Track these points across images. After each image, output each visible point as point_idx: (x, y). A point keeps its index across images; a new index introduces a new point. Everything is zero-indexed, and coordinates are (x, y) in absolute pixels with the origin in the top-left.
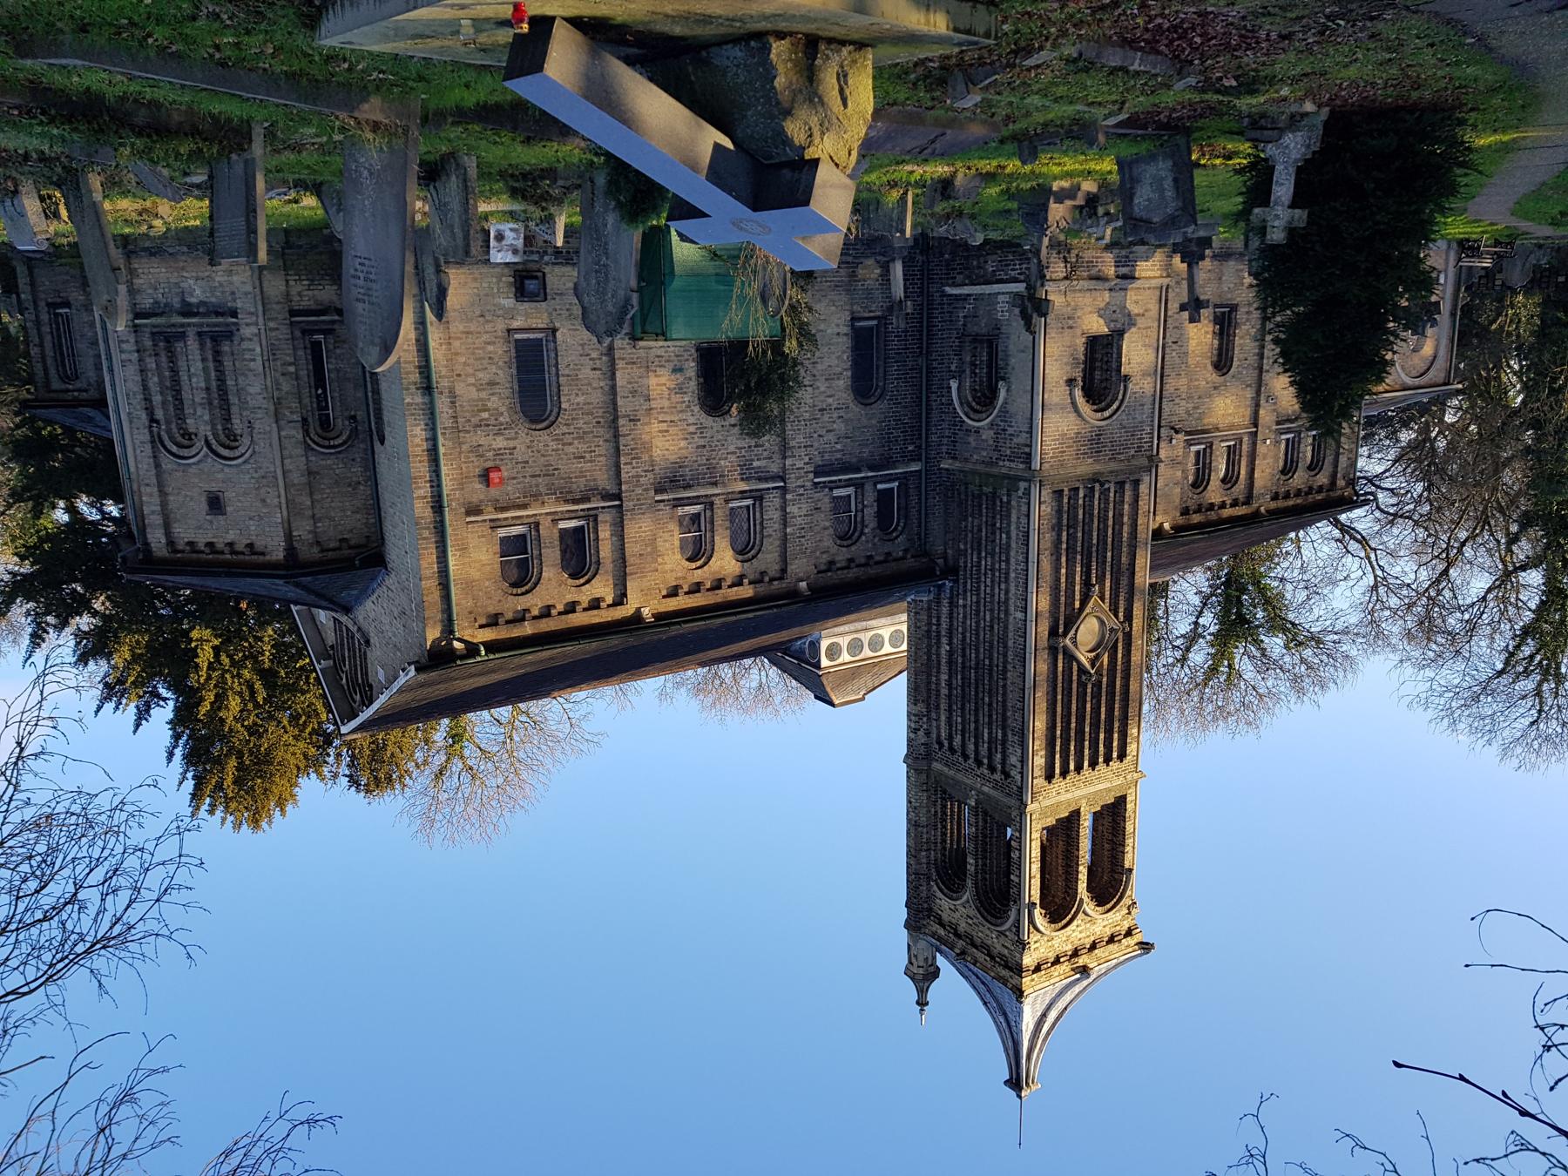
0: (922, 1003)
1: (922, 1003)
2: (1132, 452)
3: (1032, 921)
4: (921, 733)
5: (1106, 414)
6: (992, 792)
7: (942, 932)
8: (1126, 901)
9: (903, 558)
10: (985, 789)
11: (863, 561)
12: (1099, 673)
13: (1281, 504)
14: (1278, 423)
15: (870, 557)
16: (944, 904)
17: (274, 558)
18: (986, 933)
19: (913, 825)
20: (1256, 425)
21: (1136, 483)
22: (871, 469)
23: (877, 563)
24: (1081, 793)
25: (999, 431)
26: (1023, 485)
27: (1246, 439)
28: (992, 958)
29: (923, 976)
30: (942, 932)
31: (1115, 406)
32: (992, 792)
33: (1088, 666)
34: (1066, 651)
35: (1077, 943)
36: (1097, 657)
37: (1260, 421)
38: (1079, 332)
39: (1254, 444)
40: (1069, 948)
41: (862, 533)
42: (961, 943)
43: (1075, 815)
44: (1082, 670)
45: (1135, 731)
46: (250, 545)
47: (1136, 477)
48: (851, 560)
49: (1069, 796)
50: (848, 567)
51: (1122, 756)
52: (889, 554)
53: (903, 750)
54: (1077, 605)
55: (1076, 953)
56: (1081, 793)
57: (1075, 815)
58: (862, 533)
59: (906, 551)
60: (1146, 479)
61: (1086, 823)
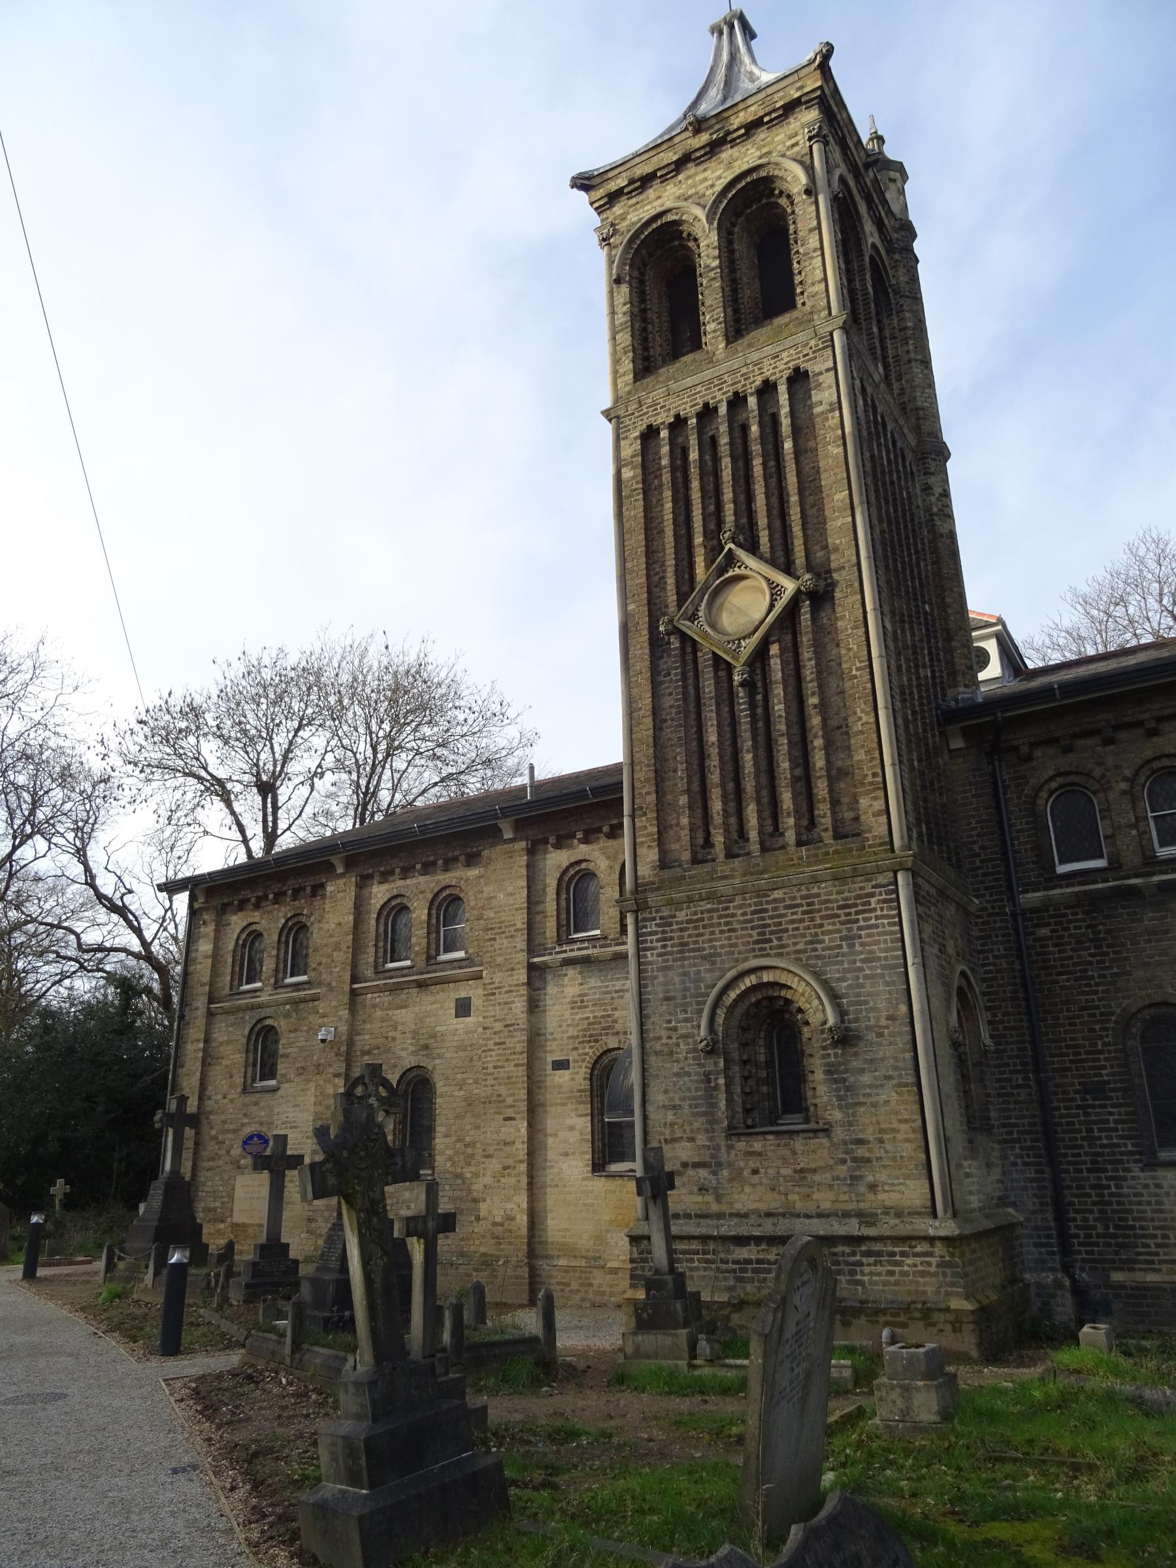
2: (682, 916)
3: (809, 169)
4: (938, 490)
5: (749, 981)
8: (620, 240)
9: (1033, 745)
11: (1122, 735)
12: (714, 549)
13: (309, 882)
14: (315, 998)
15: (1110, 741)
19: (926, 363)
20: (354, 993)
21: (664, 863)
22: (1134, 891)
23: (1096, 732)
24: (723, 368)
27: (369, 973)
31: (733, 995)
33: (741, 554)
34: (788, 569)
35: (712, 164)
36: (722, 570)
37: (346, 999)
38: (839, 1133)
39: (354, 965)
40: (727, 154)
41: (1132, 780)
43: (735, 331)
44: (753, 548)
45: (627, 473)
47: (667, 874)
48: (1153, 733)
49: (755, 356)
50: (1160, 719)
51: (649, 435)
52: (1067, 750)
53: (954, 468)
54: (774, 649)
55: (714, 148)
56: (723, 368)
57: (735, 331)
58: (1132, 780)
59: (1030, 758)
60: (645, 871)
61: (712, 322)
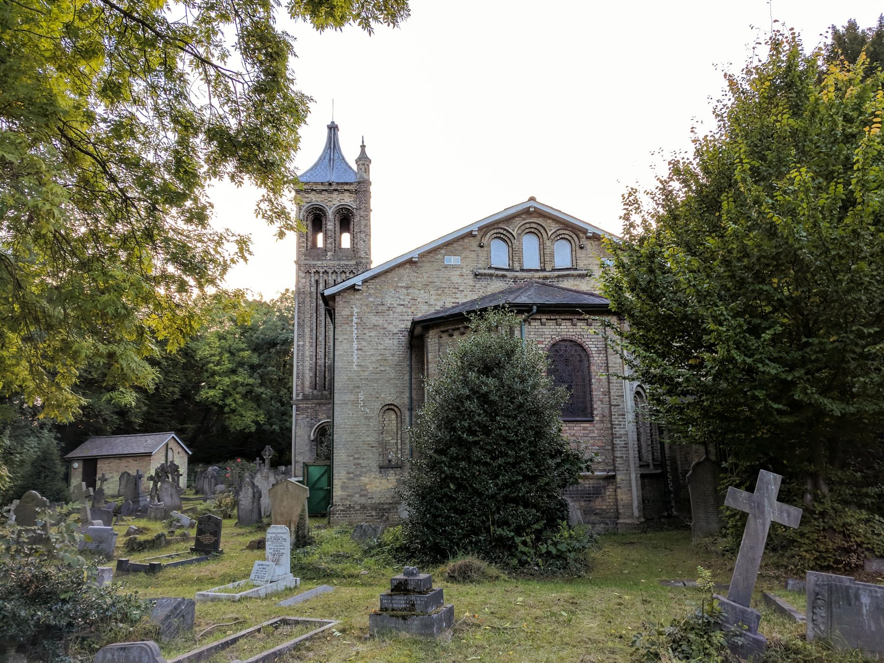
0: (363, 147)
1: (363, 147)
6: (315, 262)
7: (346, 187)
10: (320, 262)
16: (348, 200)
17: (435, 331)
18: (315, 199)
25: (316, 418)
26: (300, 397)
28: (313, 190)
29: (364, 160)
30: (346, 187)
32: (315, 262)
42: (333, 188)
46: (451, 335)
